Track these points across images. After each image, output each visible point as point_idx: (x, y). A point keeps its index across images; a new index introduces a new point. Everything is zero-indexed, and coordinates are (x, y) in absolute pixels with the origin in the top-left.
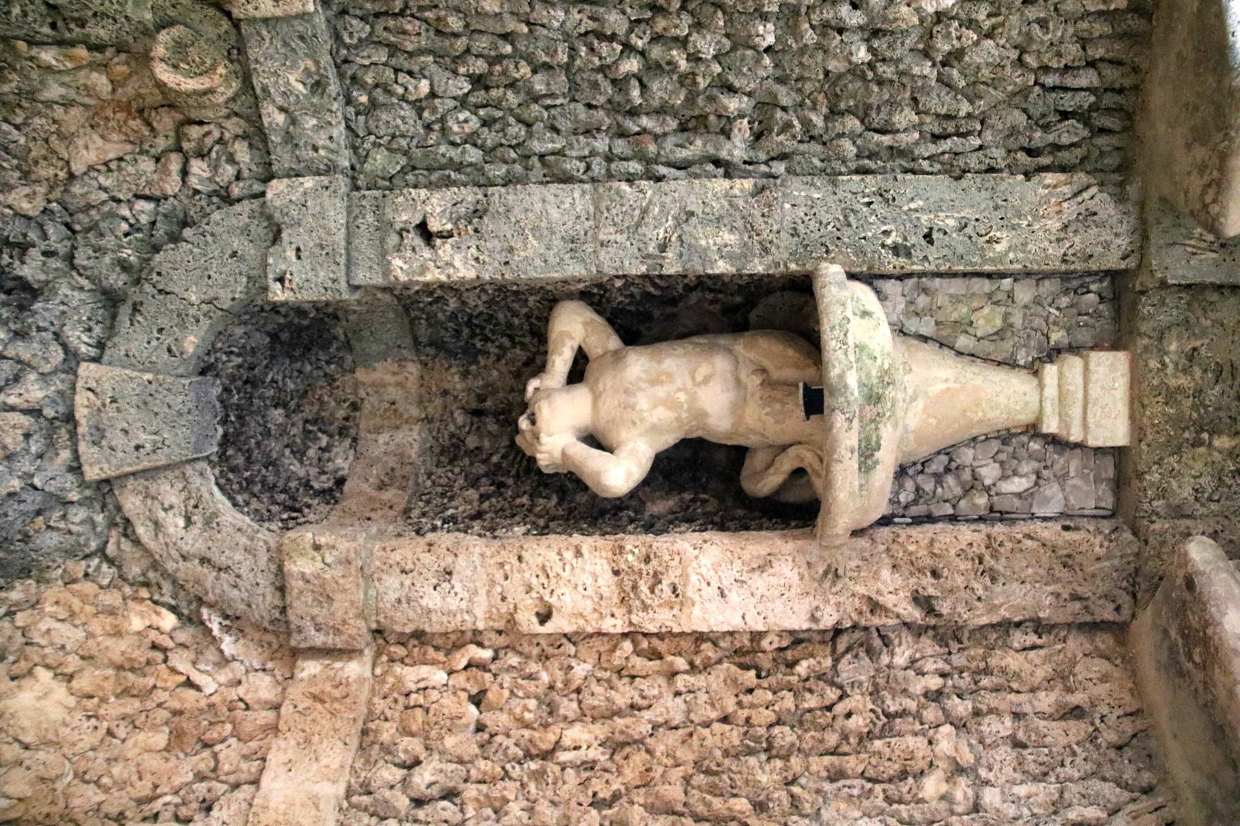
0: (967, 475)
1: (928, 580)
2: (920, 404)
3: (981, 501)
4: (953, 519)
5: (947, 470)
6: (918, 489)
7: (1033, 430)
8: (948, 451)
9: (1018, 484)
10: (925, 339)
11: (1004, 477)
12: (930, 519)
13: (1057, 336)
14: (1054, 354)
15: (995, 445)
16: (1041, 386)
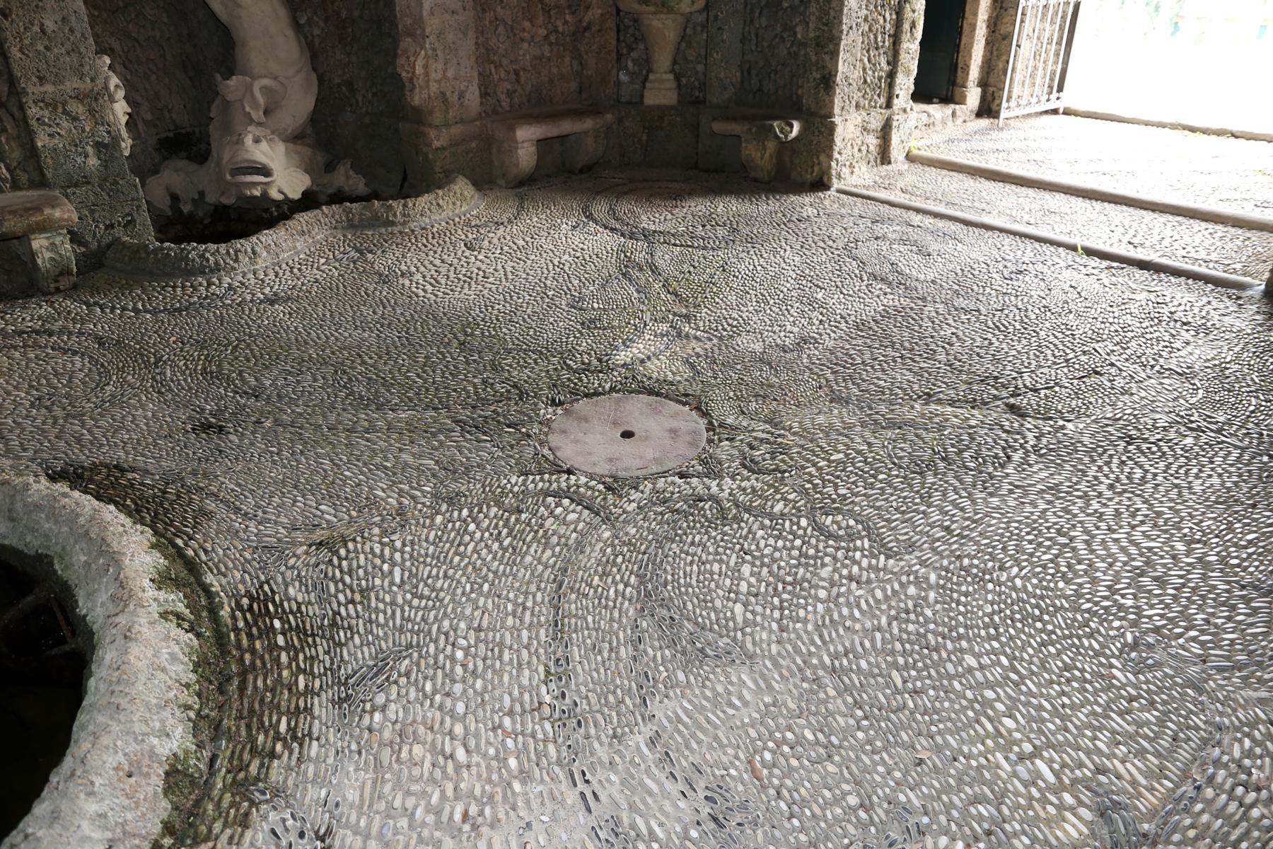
0: (634, 46)
1: (597, 28)
2: (660, 26)
3: (625, 51)
4: (618, 40)
5: (636, 39)
6: (629, 27)
7: (650, 70)
8: (643, 39)
9: (630, 64)
10: (685, 30)
11: (633, 60)
12: (618, 31)
13: (684, 80)
14: (678, 78)
15: (645, 57)
16: (666, 73)
